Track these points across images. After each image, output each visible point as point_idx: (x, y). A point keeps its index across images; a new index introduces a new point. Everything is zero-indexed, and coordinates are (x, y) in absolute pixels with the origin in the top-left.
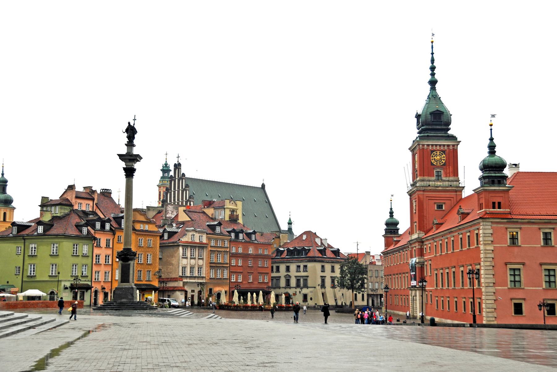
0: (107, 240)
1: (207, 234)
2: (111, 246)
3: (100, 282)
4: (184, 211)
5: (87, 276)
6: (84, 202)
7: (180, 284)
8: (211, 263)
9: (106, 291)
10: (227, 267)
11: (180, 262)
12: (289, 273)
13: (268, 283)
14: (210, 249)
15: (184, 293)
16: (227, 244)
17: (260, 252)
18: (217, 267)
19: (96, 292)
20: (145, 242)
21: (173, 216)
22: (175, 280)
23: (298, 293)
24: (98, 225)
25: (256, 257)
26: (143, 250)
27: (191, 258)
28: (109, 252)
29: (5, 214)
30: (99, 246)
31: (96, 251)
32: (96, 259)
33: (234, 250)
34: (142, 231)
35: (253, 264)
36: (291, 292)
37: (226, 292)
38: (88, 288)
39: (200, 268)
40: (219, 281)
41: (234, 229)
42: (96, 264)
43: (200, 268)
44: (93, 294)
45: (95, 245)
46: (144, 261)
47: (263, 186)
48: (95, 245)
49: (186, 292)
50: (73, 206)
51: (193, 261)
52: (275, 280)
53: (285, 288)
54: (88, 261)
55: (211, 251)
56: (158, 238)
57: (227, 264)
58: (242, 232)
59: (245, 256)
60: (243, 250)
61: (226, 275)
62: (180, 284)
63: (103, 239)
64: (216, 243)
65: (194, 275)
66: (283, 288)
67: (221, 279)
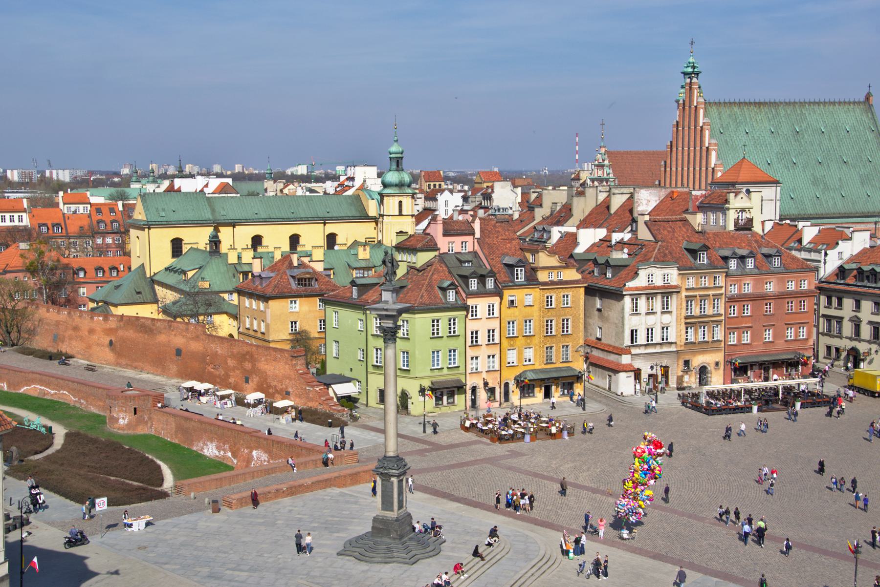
1: (679, 269)
2: (497, 314)
4: (646, 223)
5: (458, 367)
6: (458, 240)
7: (626, 359)
8: (686, 318)
9: (490, 385)
10: (721, 321)
11: (626, 322)
12: (858, 314)
13: (806, 340)
14: (684, 294)
15: (632, 374)
16: (721, 281)
17: (792, 286)
18: (699, 323)
19: (474, 390)
20: (557, 300)
21: (650, 209)
22: (620, 352)
23: (873, 351)
24: (474, 284)
25: (783, 296)
26: (553, 312)
27: (647, 314)
29: (400, 202)
31: (472, 326)
32: (472, 338)
33: (734, 290)
34: (553, 283)
35: (774, 309)
36: (862, 347)
37: (717, 364)
38: (460, 388)
40: (704, 346)
41: (734, 253)
44: (469, 392)
46: (557, 331)
47: (868, 97)
49: (637, 374)
50: (439, 249)
52: (834, 323)
53: (851, 339)
54: (457, 344)
55: (686, 297)
56: (582, 290)
57: (720, 315)
58: (752, 255)
59: (757, 298)
60: (754, 287)
61: (719, 334)
62: (626, 359)
63: (481, 304)
64: (696, 284)
65: (654, 342)
66: (847, 338)
67: (707, 342)
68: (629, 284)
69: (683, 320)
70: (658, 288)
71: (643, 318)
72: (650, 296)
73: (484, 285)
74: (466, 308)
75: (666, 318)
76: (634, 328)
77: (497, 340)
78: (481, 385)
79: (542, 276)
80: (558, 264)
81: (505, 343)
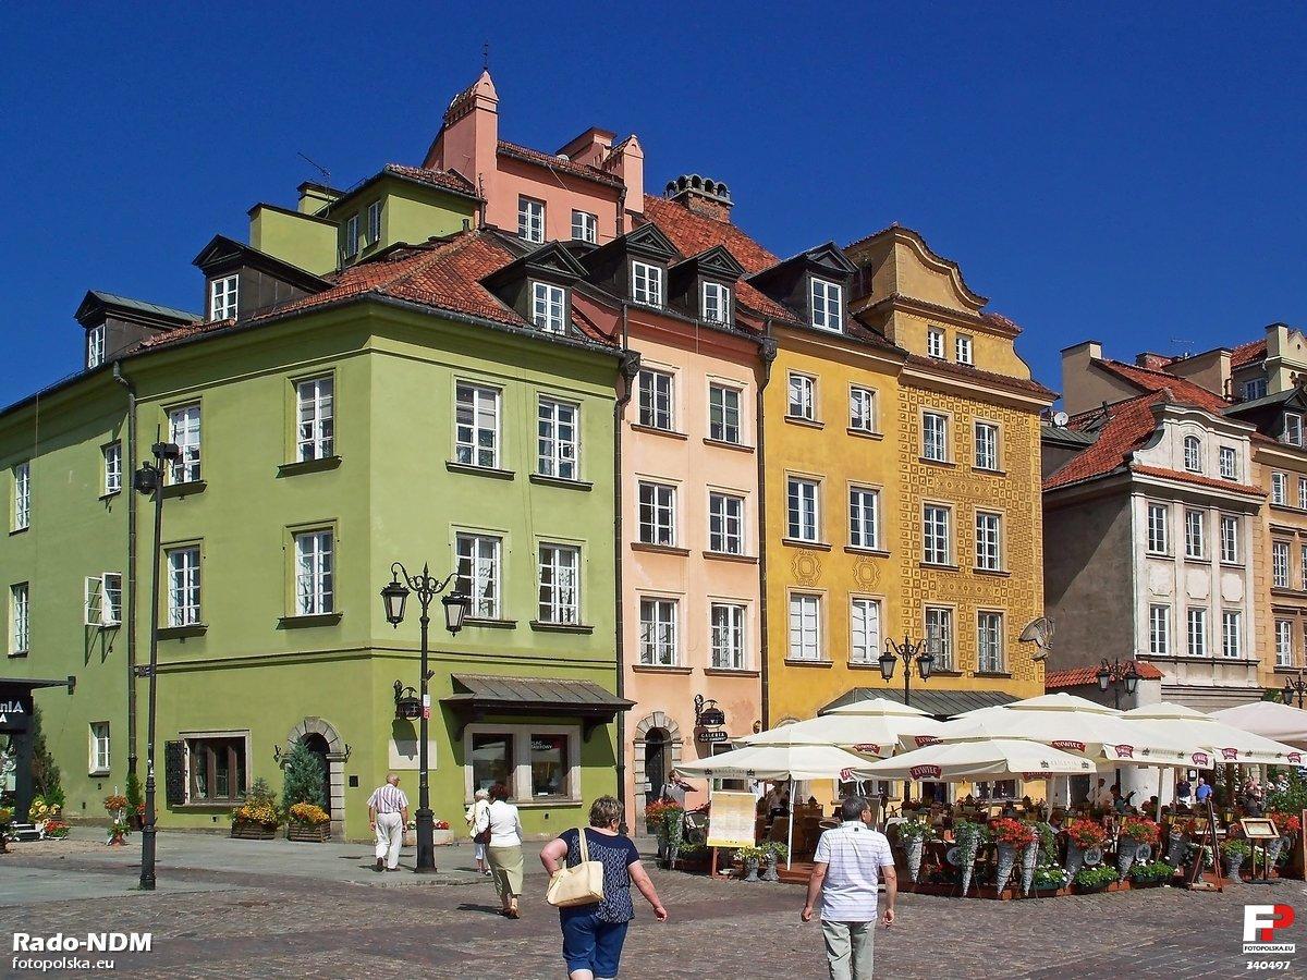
0: (716, 390)
3: (688, 671)
8: (1275, 593)
27: (1189, 562)
28: (737, 473)
30: (656, 422)
31: (645, 457)
32: (646, 514)
34: (942, 367)
39: (1230, 615)
42: (645, 542)
43: (1230, 615)
45: (633, 411)
48: (633, 411)
51: (1197, 574)
55: (1274, 530)
63: (692, 378)
68: (1142, 458)
69: (1269, 599)
70: (1216, 485)
71: (1181, 571)
72: (1197, 504)
73: (694, 309)
74: (619, 370)
75: (1232, 586)
76: (1158, 600)
77: (749, 548)
78: (686, 726)
79: (909, 333)
80: (954, 305)
81: (781, 562)
